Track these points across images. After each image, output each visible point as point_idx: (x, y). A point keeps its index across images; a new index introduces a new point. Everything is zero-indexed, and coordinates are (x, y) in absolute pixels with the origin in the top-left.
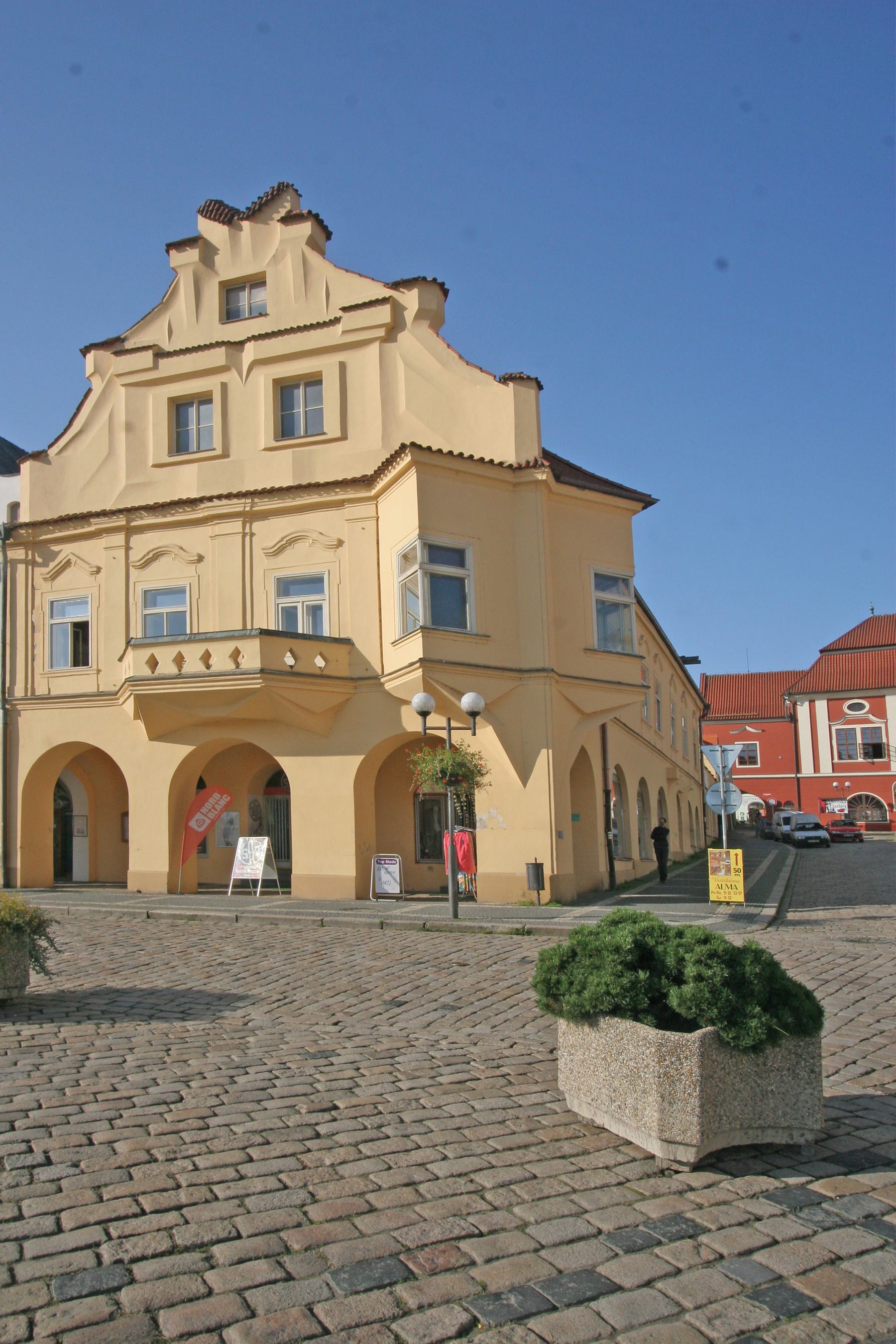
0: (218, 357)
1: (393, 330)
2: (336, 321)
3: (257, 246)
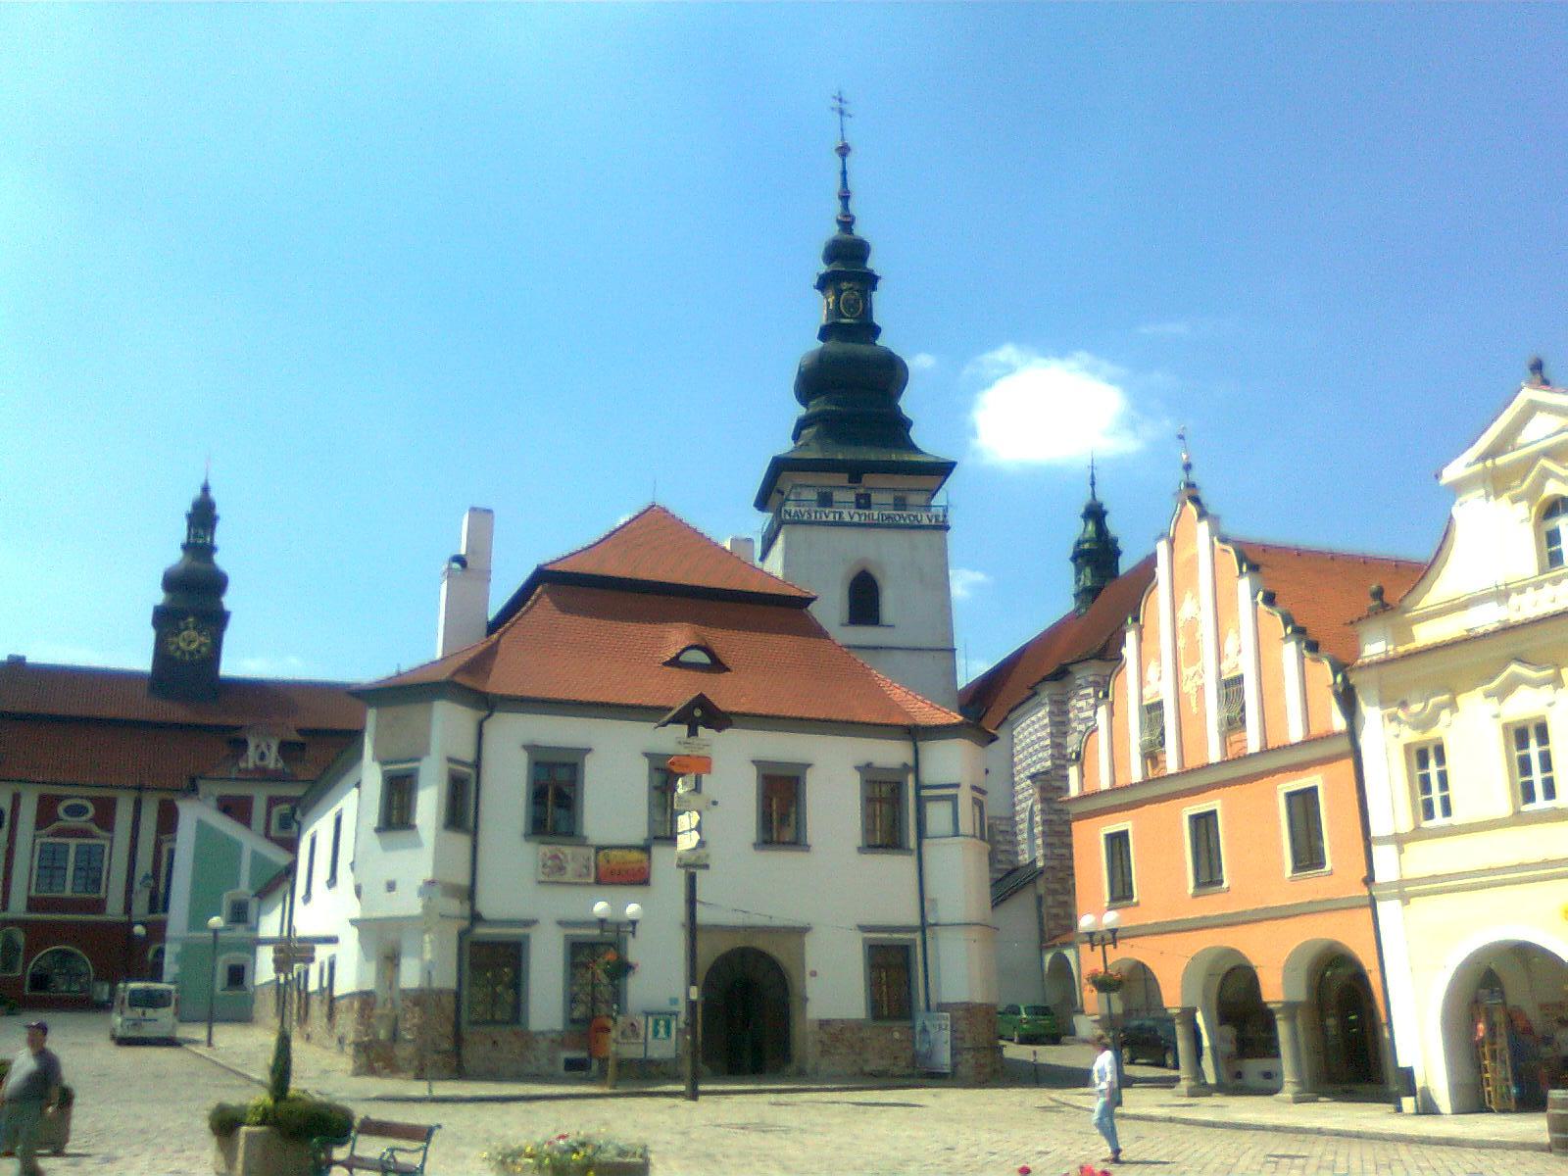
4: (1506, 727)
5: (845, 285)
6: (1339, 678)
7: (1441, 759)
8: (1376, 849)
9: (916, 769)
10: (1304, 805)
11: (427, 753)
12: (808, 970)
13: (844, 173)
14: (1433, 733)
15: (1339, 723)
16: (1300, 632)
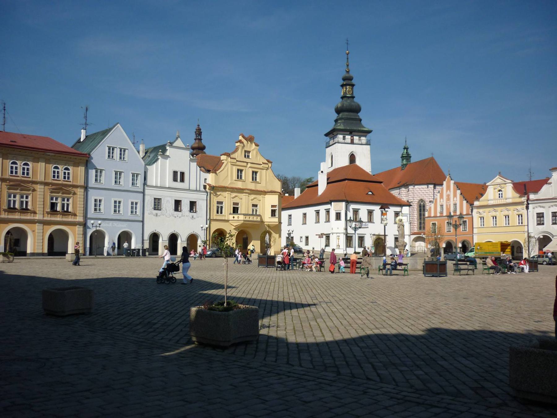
0: (245, 164)
1: (267, 169)
2: (261, 164)
3: (250, 146)
5: (348, 87)
6: (471, 207)
8: (474, 229)
9: (401, 212)
11: (343, 210)
12: (387, 241)
13: (348, 59)
15: (470, 213)
16: (466, 200)
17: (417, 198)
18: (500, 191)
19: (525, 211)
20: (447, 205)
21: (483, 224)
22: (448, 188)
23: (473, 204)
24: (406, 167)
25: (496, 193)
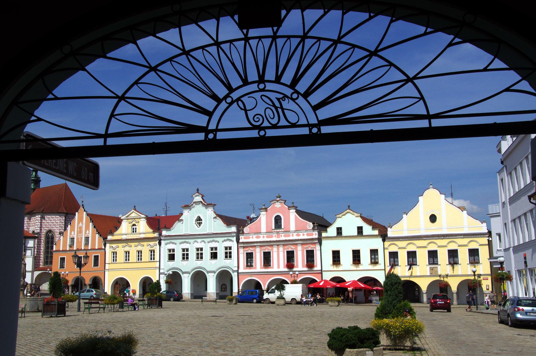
4: (125, 251)
6: (104, 241)
7: (116, 254)
8: (106, 264)
10: (96, 258)
14: (115, 251)
15: (103, 247)
16: (99, 233)
17: (45, 229)
18: (134, 225)
19: (158, 246)
20: (78, 239)
21: (116, 260)
22: (80, 220)
23: (107, 238)
24: (33, 192)
25: (130, 227)
